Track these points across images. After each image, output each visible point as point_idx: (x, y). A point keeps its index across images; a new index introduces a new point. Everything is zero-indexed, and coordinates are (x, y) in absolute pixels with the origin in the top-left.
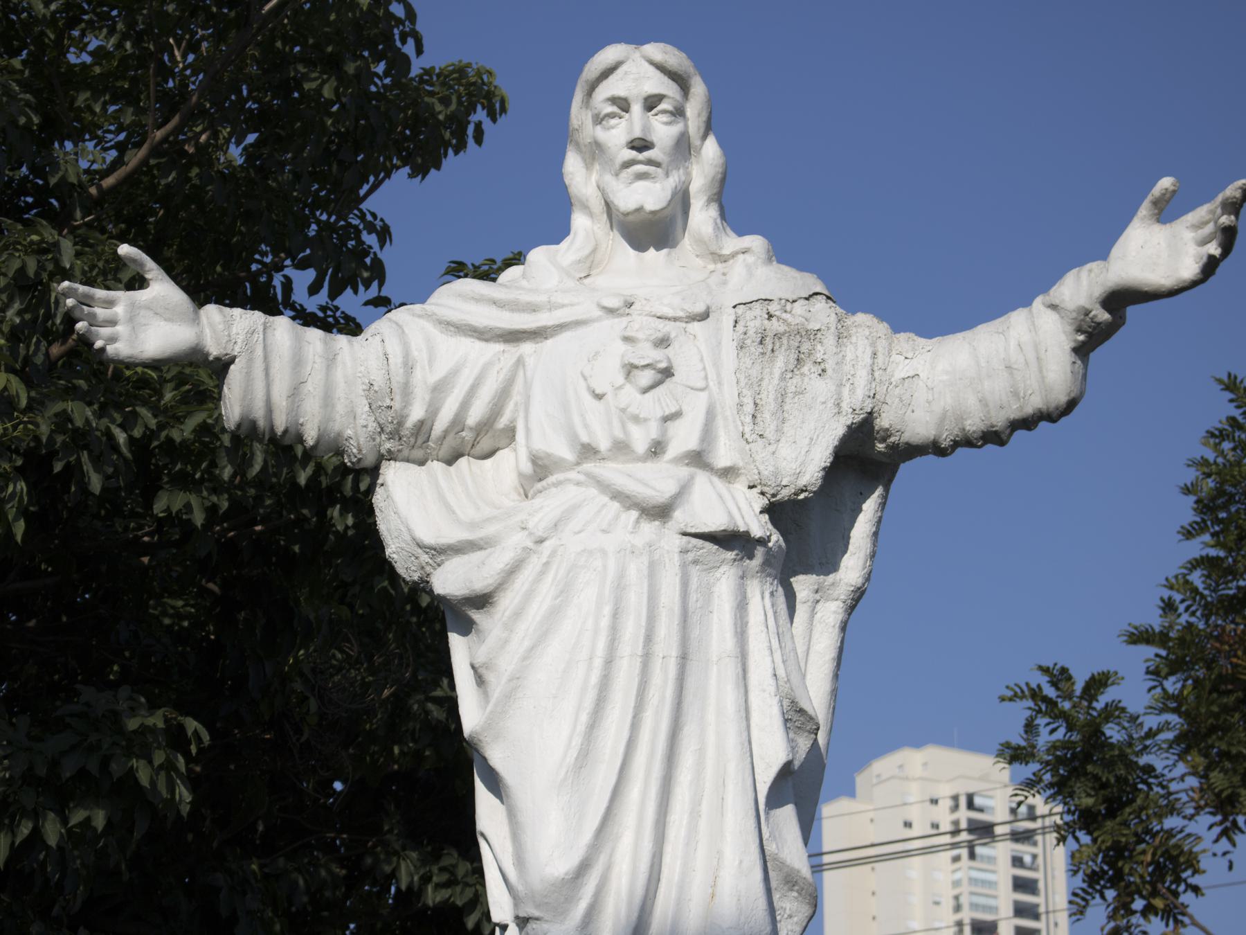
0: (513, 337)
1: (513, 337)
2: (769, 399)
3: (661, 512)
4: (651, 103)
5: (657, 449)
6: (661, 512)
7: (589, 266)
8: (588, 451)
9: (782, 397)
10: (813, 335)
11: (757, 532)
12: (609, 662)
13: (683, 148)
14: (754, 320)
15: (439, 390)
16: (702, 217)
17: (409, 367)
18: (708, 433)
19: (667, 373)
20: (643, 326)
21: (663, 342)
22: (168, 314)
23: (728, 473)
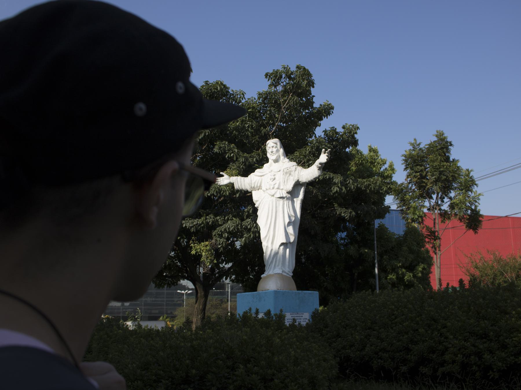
0: (261, 176)
1: (261, 176)
2: (286, 181)
3: (273, 196)
4: (273, 147)
5: (273, 188)
6: (273, 196)
7: (271, 165)
8: (267, 189)
9: (287, 180)
10: (292, 171)
11: (284, 196)
12: (268, 213)
13: (278, 151)
14: (285, 171)
15: (254, 183)
16: (282, 157)
17: (251, 181)
18: (279, 185)
19: (274, 179)
20: (273, 173)
21: (274, 175)
22: (226, 179)
23: (282, 189)
